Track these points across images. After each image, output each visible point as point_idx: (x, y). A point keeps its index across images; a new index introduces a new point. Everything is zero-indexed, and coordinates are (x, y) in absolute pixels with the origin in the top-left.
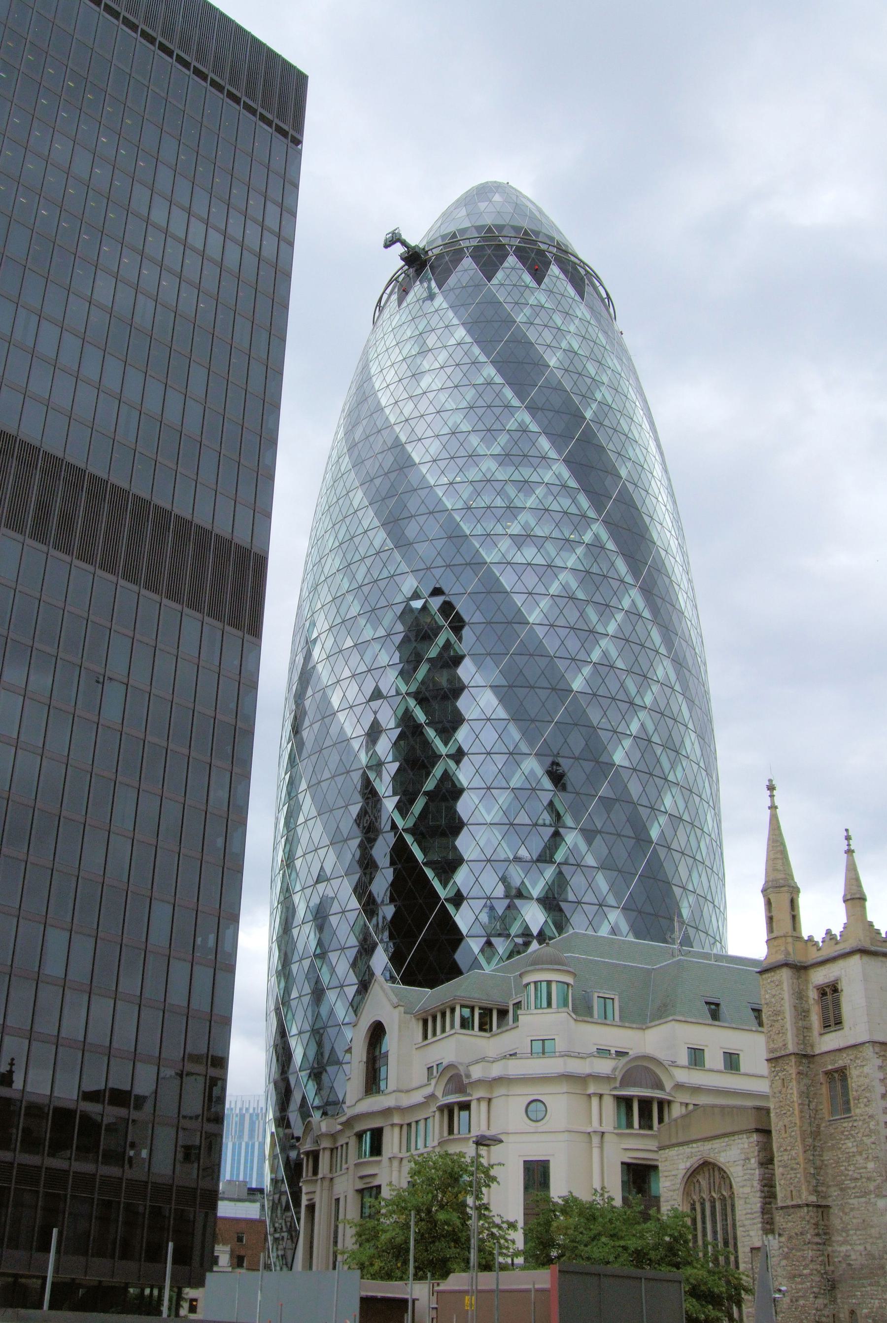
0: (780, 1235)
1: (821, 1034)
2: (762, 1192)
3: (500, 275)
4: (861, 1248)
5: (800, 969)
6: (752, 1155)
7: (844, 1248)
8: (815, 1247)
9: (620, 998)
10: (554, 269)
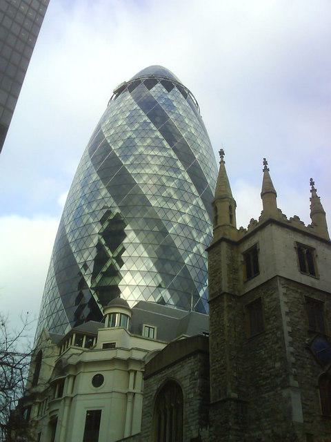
0: (211, 426)
1: (245, 282)
2: (200, 395)
3: (154, 89)
4: (270, 431)
5: (234, 244)
6: (196, 369)
7: (258, 433)
8: (234, 433)
9: (158, 329)
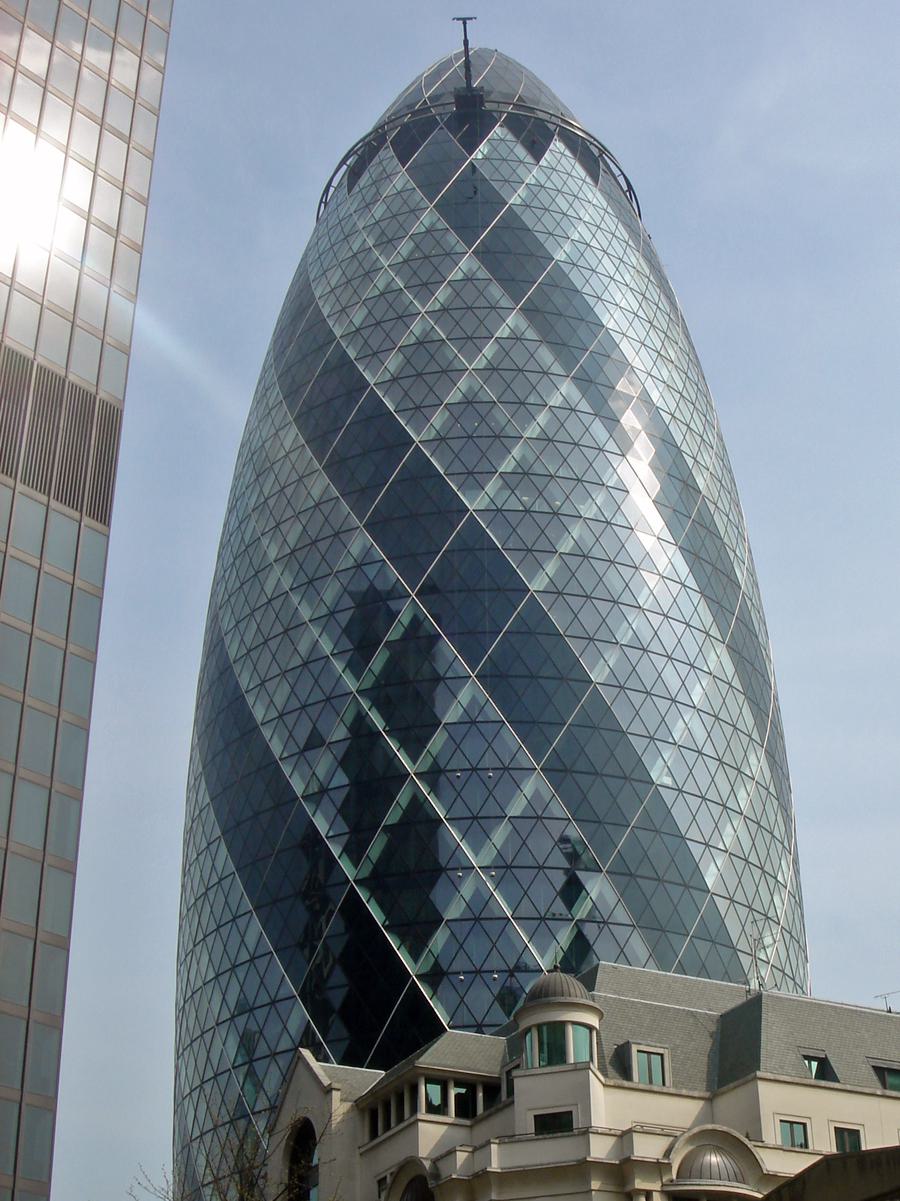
10: (557, 145)
